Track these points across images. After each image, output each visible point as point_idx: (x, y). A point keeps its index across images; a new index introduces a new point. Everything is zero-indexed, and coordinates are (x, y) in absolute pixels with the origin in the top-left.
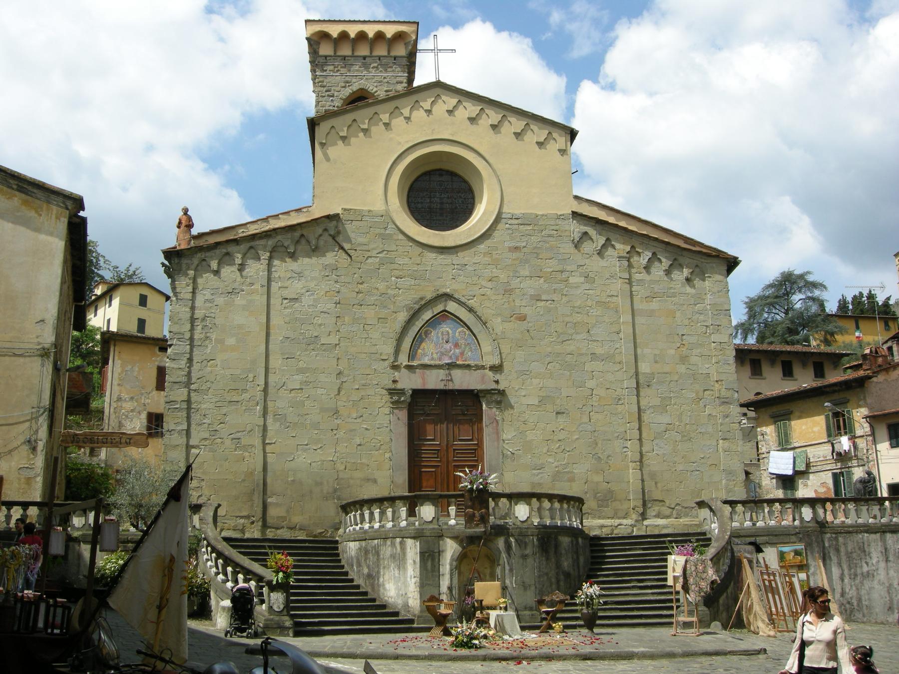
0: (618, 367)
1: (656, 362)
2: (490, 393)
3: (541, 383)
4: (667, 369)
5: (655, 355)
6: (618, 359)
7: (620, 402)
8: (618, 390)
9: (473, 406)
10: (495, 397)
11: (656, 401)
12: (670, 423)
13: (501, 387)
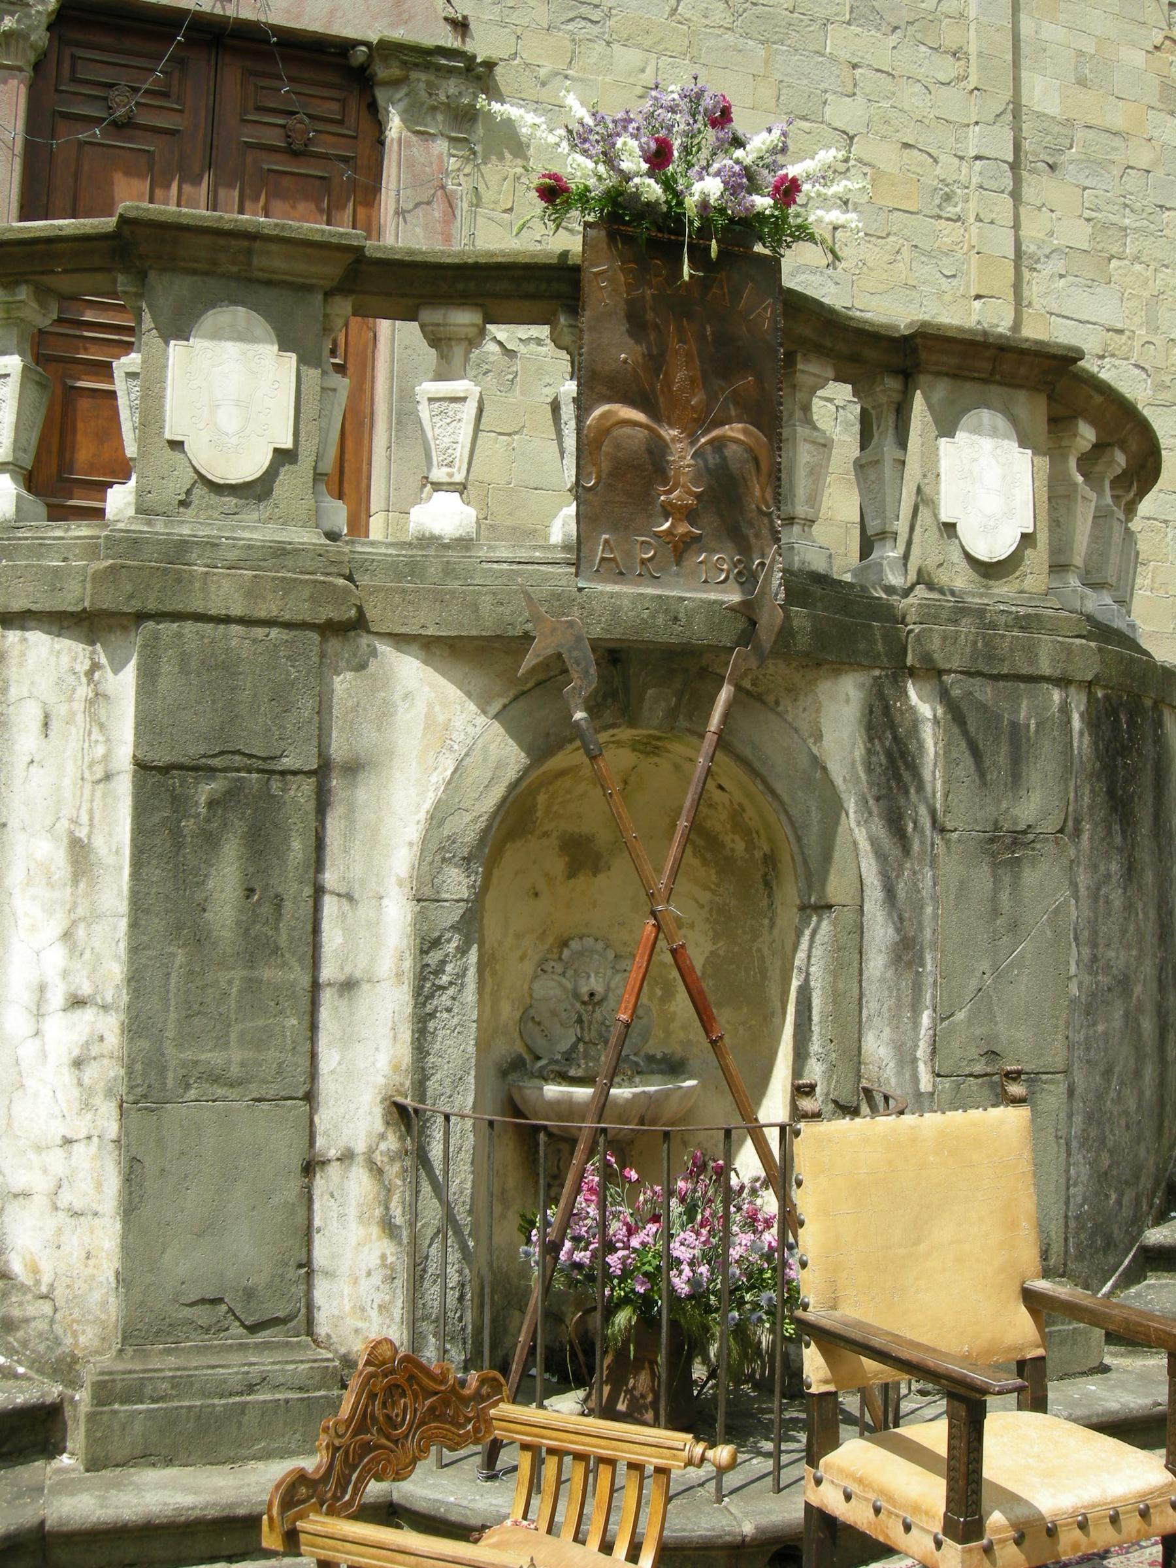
0: (947, 68)
1: (1082, 82)
2: (427, 67)
3: (650, 70)
4: (1116, 118)
5: (1081, 53)
6: (951, 37)
7: (951, 210)
8: (943, 158)
9: (341, 123)
10: (452, 86)
11: (1078, 235)
12: (1119, 326)
13: (480, 47)
